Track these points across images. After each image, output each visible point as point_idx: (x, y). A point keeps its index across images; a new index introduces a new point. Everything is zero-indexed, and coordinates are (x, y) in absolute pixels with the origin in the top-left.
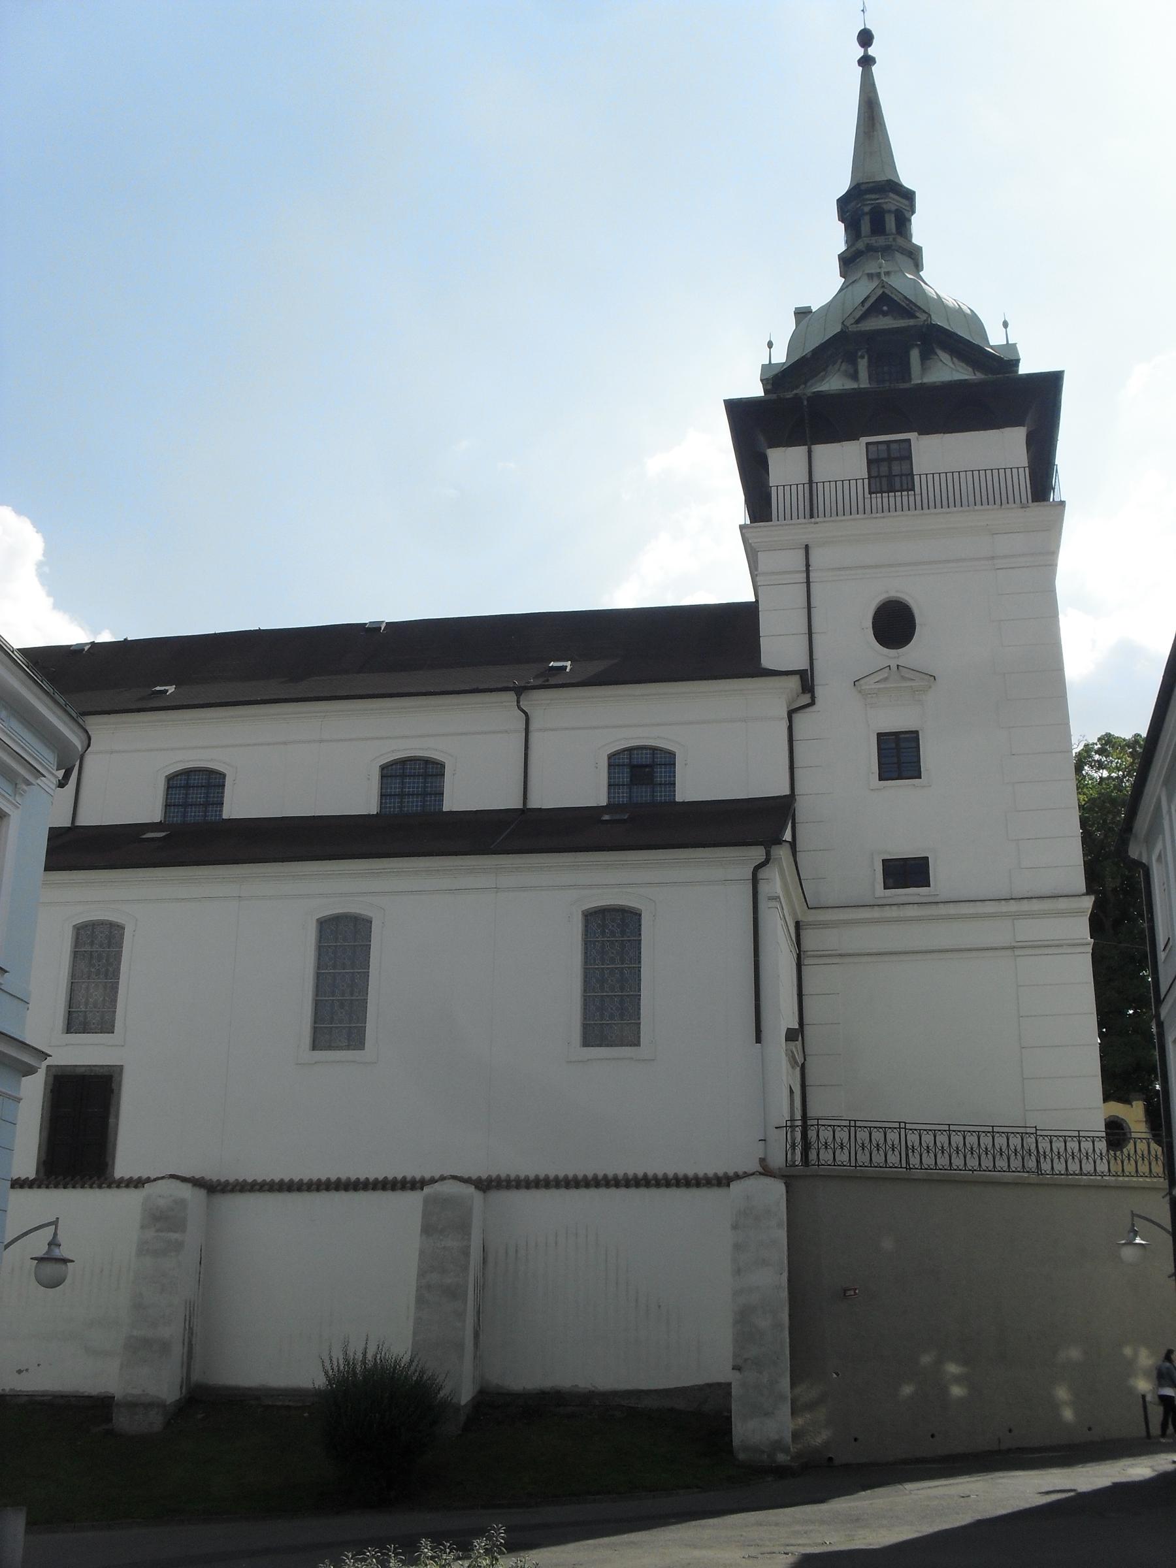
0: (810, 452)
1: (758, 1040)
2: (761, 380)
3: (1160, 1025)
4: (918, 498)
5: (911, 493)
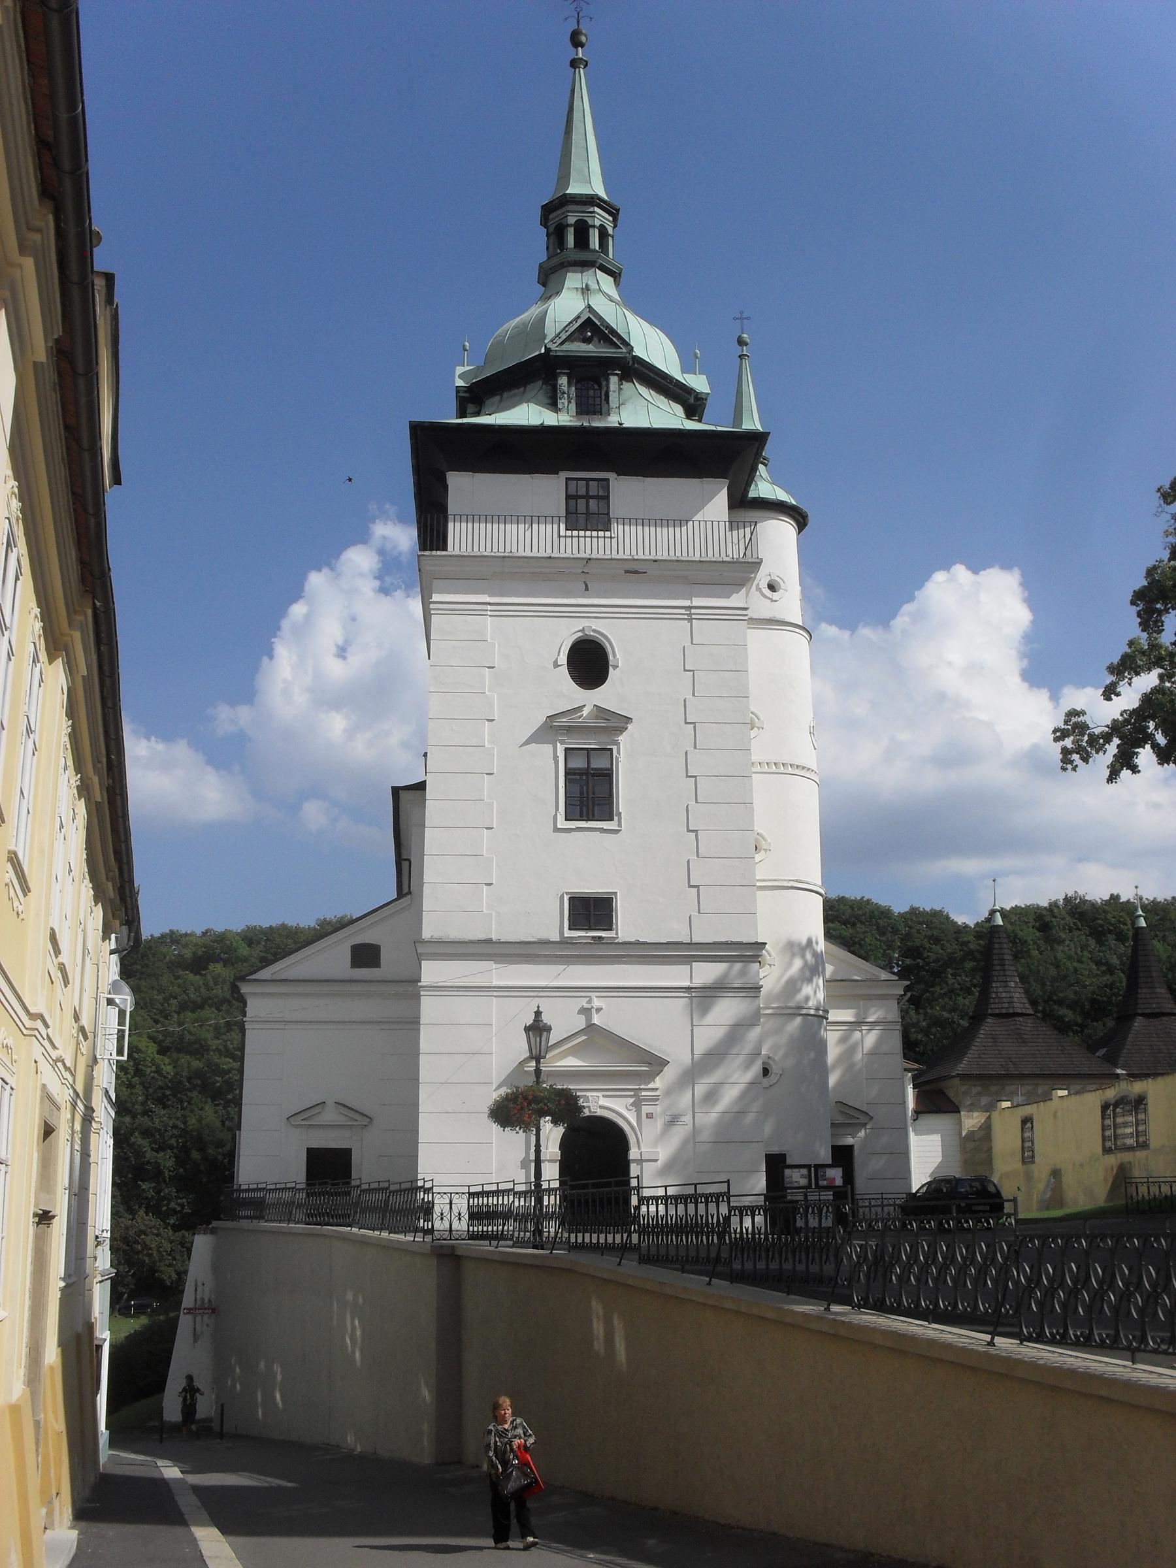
5: (608, 534)
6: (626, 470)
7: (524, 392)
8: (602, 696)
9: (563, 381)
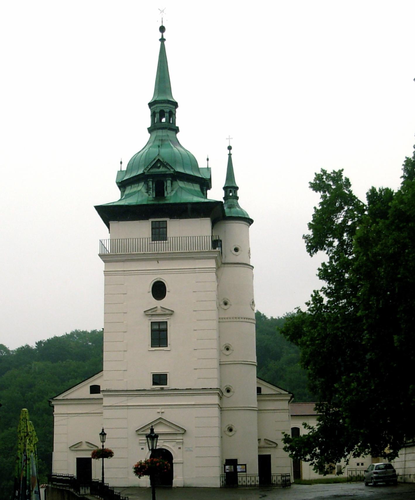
2: (117, 183)
4: (169, 244)
7: (138, 186)
8: (164, 303)
9: (150, 183)
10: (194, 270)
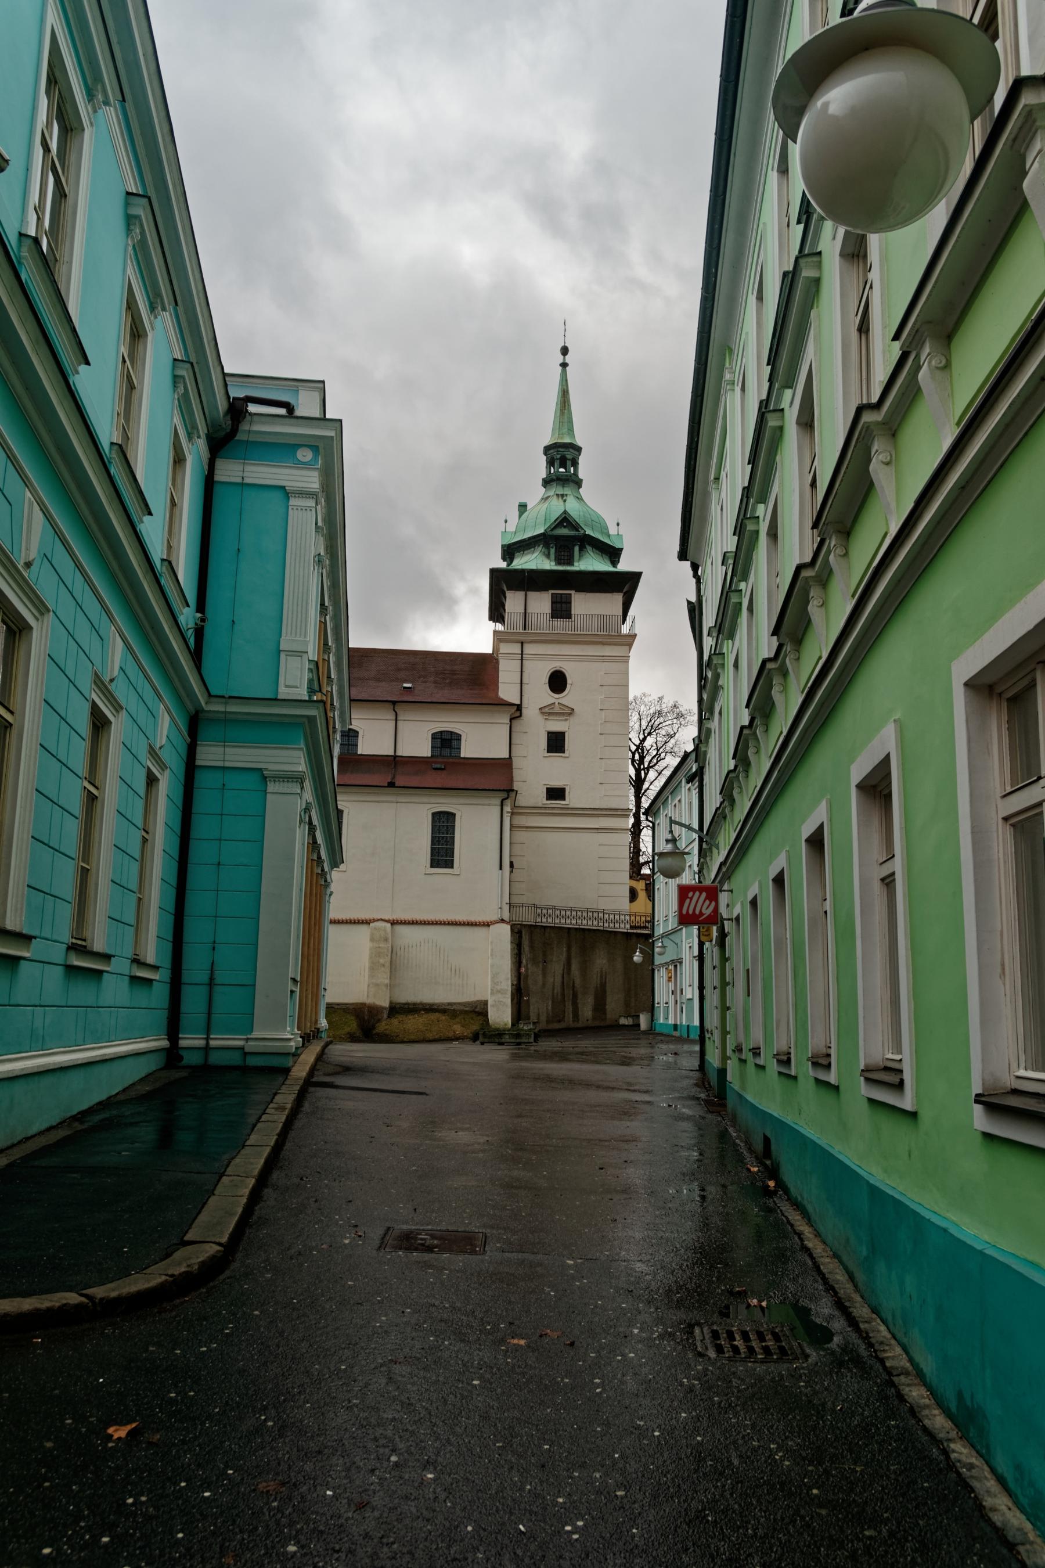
0: (526, 595)
1: (501, 869)
3: (654, 880)
6: (580, 589)
8: (567, 698)
10: (603, 659)
